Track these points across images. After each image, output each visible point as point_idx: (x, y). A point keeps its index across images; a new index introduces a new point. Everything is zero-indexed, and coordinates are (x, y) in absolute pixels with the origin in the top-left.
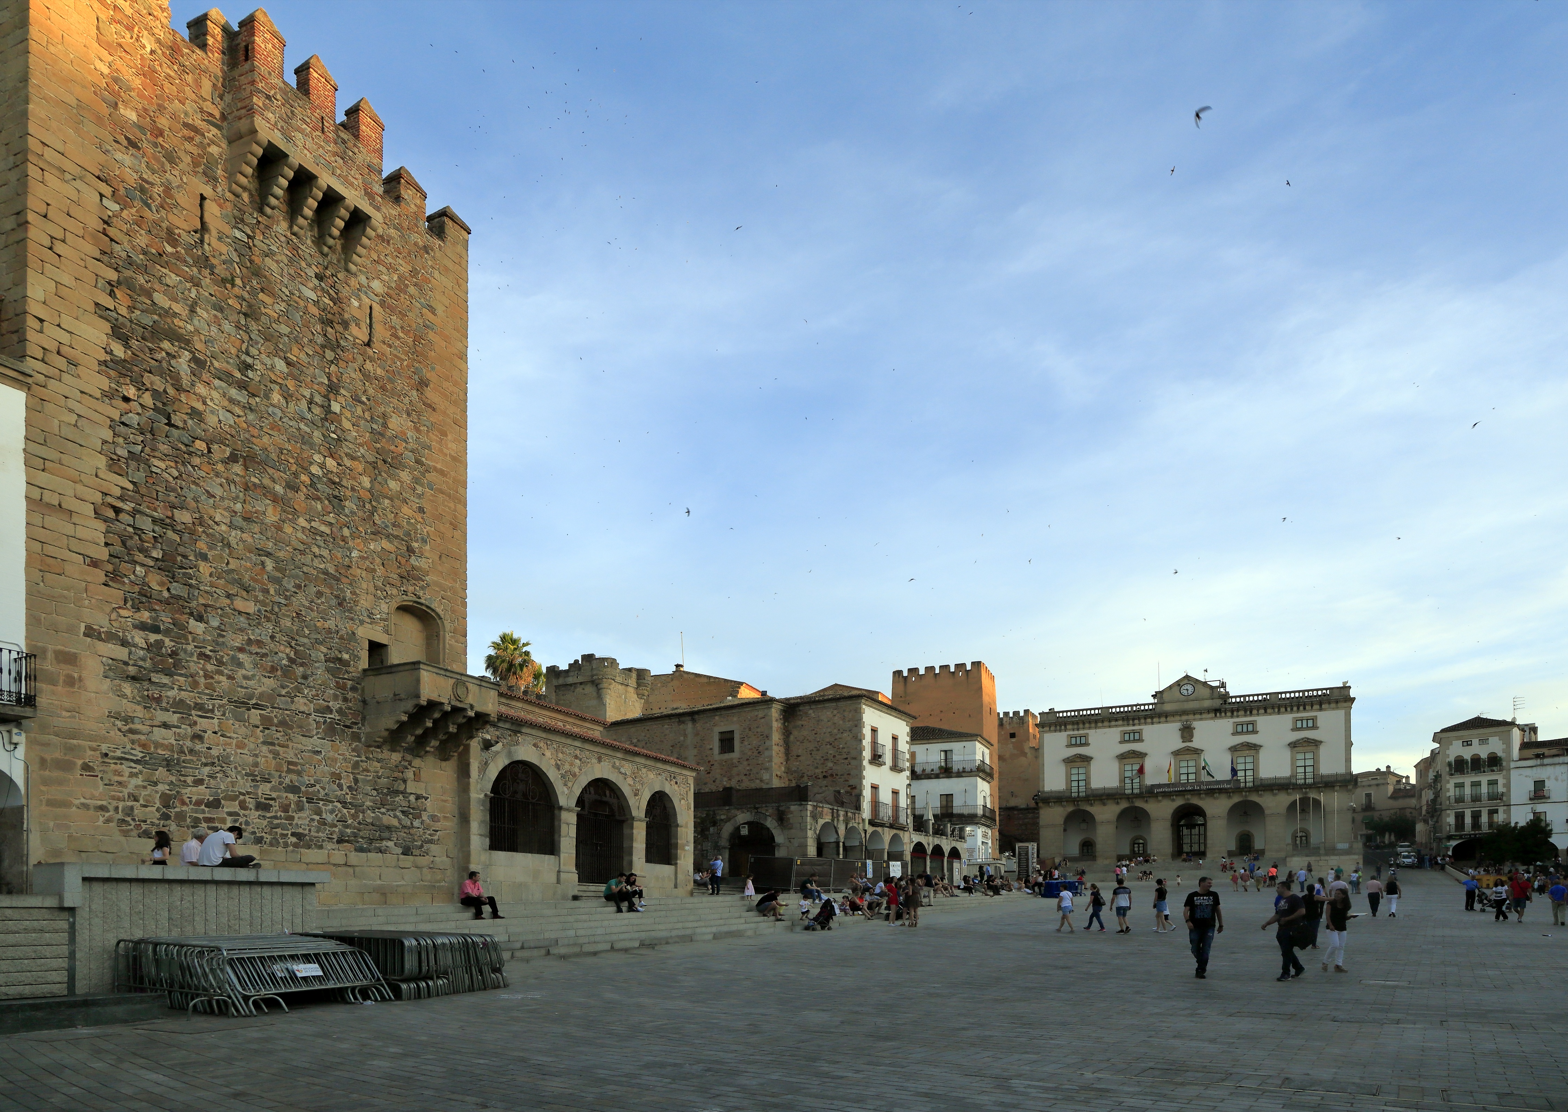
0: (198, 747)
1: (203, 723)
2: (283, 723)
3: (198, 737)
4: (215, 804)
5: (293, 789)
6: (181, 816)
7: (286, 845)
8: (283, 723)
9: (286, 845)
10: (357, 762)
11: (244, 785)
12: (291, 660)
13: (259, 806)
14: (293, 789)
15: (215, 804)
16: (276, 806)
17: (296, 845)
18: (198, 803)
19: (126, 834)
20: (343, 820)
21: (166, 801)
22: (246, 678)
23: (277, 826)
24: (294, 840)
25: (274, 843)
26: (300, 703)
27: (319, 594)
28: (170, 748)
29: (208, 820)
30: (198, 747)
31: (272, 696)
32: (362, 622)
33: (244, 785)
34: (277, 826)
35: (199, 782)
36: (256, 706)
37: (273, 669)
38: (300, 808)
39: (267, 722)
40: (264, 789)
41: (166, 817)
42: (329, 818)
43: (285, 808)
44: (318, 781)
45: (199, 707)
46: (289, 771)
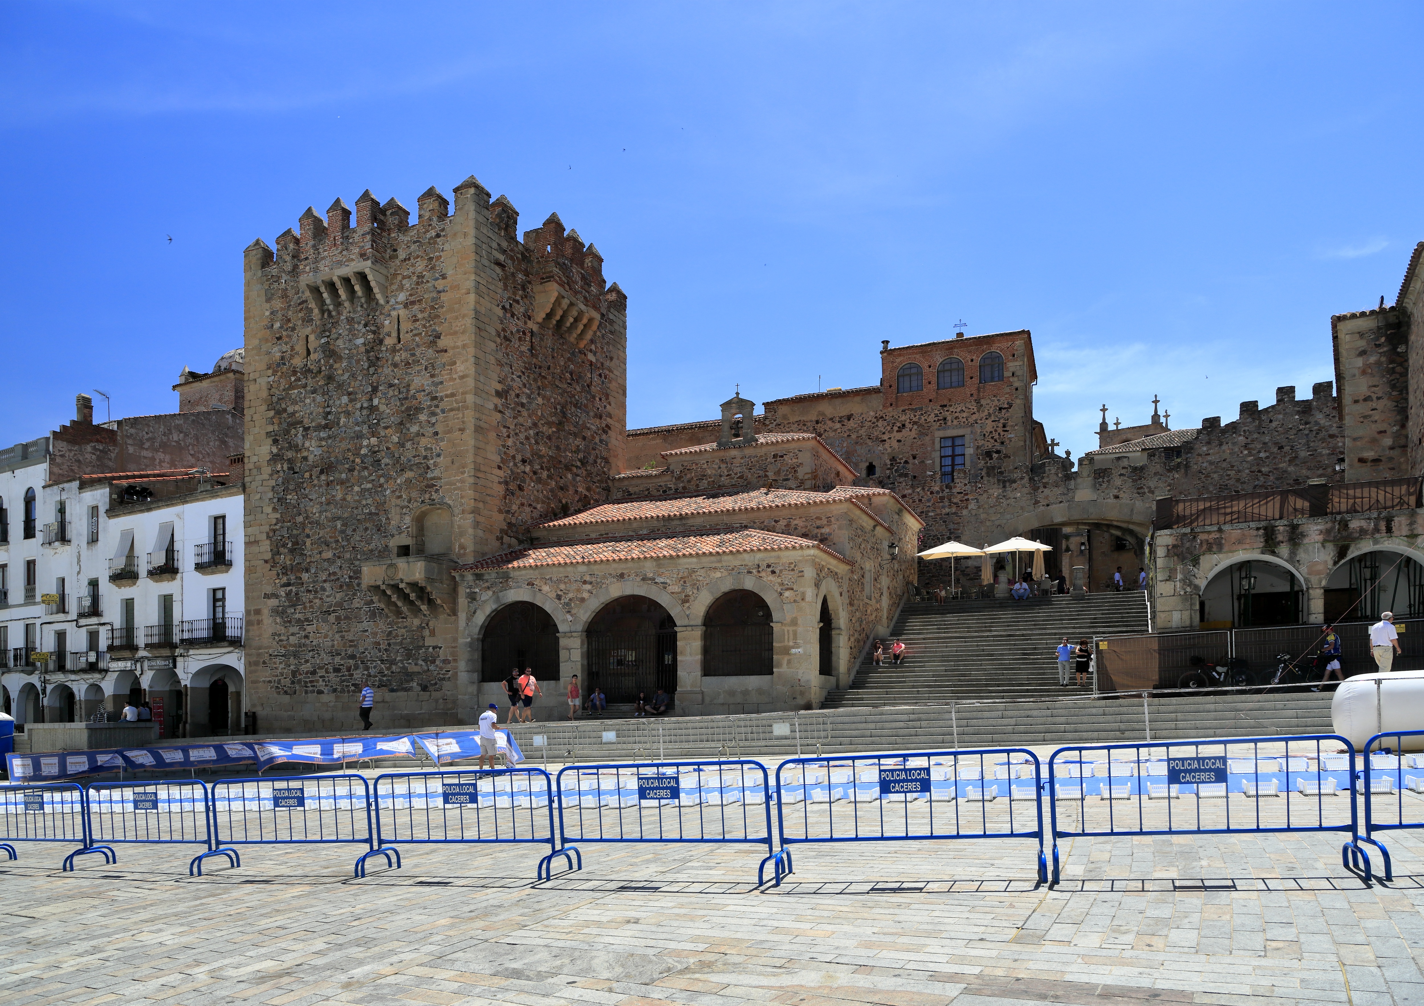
0: (308, 642)
1: (309, 629)
2: (347, 618)
3: (306, 637)
4: (314, 673)
5: (353, 657)
6: (299, 681)
7: (349, 691)
8: (347, 618)
9: (349, 691)
10: (390, 632)
11: (327, 659)
12: (350, 577)
13: (337, 670)
14: (353, 657)
15: (314, 673)
16: (344, 669)
17: (354, 691)
18: (307, 673)
19: (279, 693)
20: (381, 672)
21: (294, 673)
22: (328, 596)
23: (344, 681)
24: (353, 688)
25: (343, 691)
26: (357, 603)
27: (366, 529)
28: (295, 646)
29: (311, 682)
30: (308, 642)
31: (340, 604)
32: (393, 536)
33: (327, 659)
34: (344, 681)
35: (307, 661)
36: (334, 611)
37: (341, 587)
38: (357, 667)
39: (338, 619)
40: (337, 659)
41: (293, 683)
42: (372, 671)
43: (349, 669)
44: (366, 649)
45: (307, 620)
46: (351, 646)
